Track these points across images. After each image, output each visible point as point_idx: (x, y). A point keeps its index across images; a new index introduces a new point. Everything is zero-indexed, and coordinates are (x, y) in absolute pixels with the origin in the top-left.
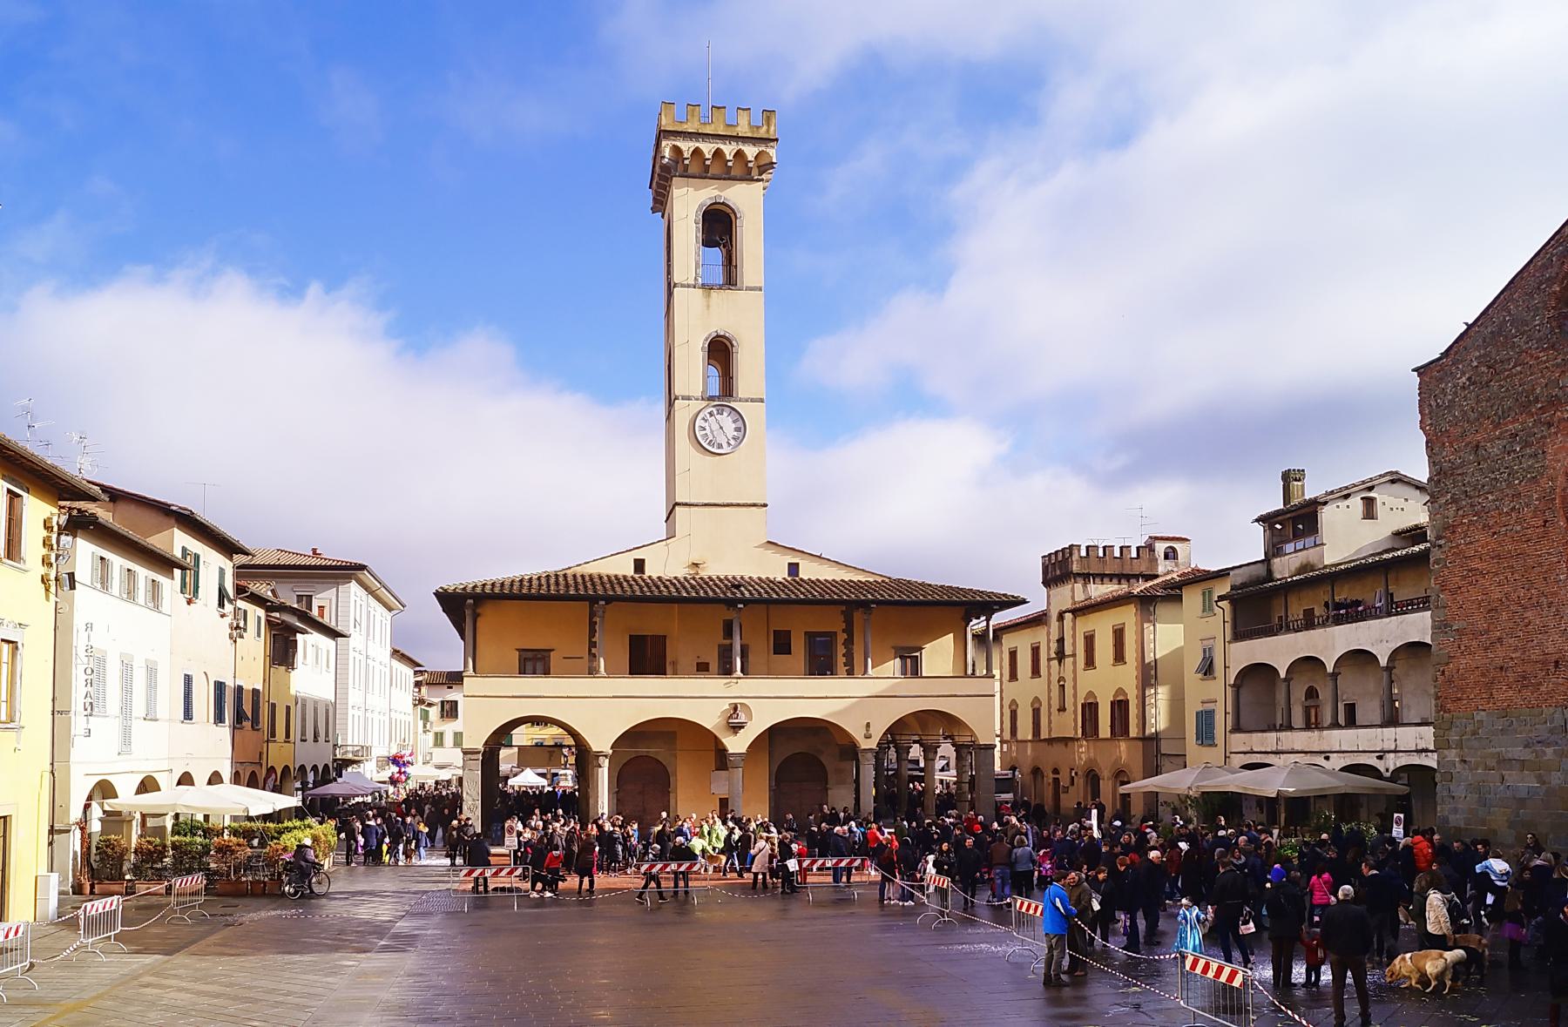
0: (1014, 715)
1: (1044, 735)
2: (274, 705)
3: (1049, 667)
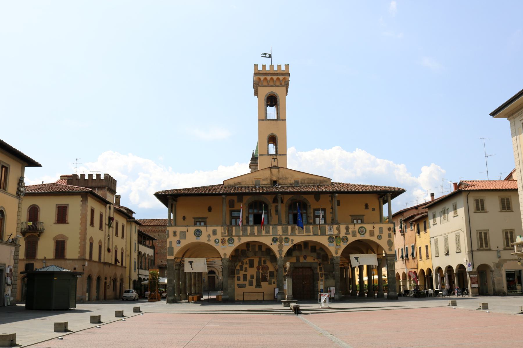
0: (91, 244)
1: (102, 261)
2: (420, 248)
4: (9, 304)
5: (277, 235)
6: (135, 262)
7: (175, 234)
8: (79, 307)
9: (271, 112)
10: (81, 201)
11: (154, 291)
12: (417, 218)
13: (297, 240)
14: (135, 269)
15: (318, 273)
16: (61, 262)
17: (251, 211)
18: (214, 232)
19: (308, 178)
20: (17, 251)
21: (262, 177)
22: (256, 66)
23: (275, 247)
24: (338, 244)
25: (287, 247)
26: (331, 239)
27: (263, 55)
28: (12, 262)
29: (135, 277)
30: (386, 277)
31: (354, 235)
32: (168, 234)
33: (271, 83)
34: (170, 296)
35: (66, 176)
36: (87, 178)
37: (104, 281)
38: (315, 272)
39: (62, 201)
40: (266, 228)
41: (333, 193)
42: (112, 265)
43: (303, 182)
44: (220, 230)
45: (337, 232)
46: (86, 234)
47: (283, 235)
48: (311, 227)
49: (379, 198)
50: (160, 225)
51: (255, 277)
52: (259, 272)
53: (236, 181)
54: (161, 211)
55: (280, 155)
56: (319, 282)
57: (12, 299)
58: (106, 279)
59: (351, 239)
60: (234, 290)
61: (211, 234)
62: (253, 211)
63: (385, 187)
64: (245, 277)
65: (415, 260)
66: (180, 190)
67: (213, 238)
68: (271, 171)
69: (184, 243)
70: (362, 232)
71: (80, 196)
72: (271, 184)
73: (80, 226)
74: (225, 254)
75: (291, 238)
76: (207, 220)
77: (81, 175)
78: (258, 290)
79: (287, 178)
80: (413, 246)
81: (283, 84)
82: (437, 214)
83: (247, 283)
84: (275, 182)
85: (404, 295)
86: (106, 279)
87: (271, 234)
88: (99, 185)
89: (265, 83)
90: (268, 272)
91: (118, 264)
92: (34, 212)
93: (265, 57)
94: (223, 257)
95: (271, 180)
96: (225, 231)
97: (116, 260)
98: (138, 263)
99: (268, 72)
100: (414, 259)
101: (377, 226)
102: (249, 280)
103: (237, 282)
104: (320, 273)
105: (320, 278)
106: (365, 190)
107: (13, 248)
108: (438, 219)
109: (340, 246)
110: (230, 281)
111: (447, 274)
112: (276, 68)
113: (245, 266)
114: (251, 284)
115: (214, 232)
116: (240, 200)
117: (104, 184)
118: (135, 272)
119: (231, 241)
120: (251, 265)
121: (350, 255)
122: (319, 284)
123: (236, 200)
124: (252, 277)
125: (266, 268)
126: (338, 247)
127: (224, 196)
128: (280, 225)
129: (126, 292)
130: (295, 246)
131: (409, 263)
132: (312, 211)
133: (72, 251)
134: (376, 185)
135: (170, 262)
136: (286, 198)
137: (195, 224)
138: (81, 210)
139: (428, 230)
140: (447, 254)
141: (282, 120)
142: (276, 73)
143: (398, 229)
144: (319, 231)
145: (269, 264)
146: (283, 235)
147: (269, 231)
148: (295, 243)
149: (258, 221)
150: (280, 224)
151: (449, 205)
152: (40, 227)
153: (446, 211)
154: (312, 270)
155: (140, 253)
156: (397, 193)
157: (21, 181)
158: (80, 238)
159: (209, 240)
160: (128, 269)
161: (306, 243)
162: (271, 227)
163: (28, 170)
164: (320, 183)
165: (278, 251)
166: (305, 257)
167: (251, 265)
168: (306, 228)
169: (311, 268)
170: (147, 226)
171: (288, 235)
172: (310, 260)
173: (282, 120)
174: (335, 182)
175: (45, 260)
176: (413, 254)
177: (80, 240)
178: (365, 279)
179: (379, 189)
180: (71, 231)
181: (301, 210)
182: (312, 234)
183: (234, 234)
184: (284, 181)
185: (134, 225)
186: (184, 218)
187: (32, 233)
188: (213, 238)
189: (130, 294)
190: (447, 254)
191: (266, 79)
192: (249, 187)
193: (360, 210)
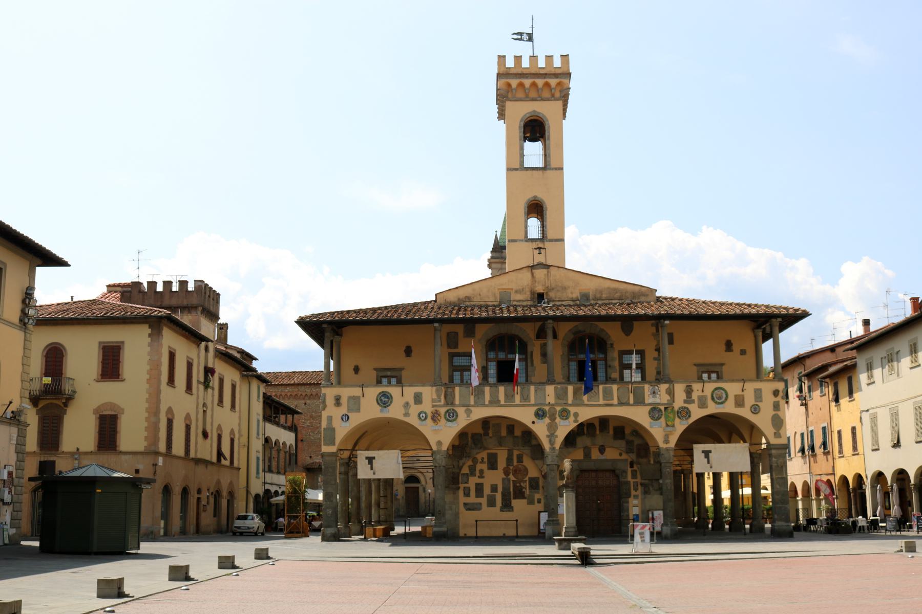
0: (170, 422)
1: (192, 455)
2: (839, 432)
3: (198, 391)
4: (7, 541)
5: (545, 404)
6: (258, 459)
7: (338, 401)
8: (146, 547)
9: (533, 152)
10: (150, 335)
11: (296, 518)
12: (834, 370)
13: (587, 413)
14: (258, 473)
15: (628, 483)
16: (108, 458)
17: (492, 355)
18: (418, 399)
19: (609, 288)
20: (22, 436)
21: (514, 287)
22: (502, 58)
23: (540, 429)
24: (669, 423)
25: (564, 428)
26: (655, 413)
27: (515, 37)
28: (13, 458)
29: (257, 488)
30: (769, 491)
31: (703, 405)
32: (324, 402)
33: (533, 94)
34: (329, 526)
35: (119, 285)
36: (160, 288)
37: (196, 496)
38: (622, 480)
39: (112, 335)
40: (522, 389)
41: (659, 318)
42: (212, 463)
43: (598, 296)
44: (428, 393)
45: (668, 398)
46: (158, 401)
47: (557, 404)
48: (615, 387)
49: (754, 330)
50: (307, 384)
51: (500, 489)
52: (509, 480)
53: (462, 294)
54: (310, 356)
55: (551, 241)
56: (630, 500)
57: (13, 531)
58: (199, 491)
59: (697, 413)
60: (457, 515)
61: (412, 402)
62: (497, 355)
63: (767, 307)
64: (479, 489)
65: (830, 457)
66: (348, 312)
67: (414, 409)
68: (532, 274)
69: (357, 419)
70: (720, 398)
71: (147, 326)
72: (532, 299)
73: (147, 386)
74: (439, 443)
75: (573, 410)
76: (404, 373)
77: (149, 283)
78: (507, 515)
79: (564, 288)
80: (824, 428)
81: (557, 95)
82: (876, 361)
83: (484, 501)
84: (541, 296)
85: (806, 529)
86: (199, 491)
87: (533, 402)
88: (185, 303)
89: (520, 94)
90: (527, 479)
91: (223, 462)
92: (54, 358)
93: (521, 39)
94: (435, 448)
95: (532, 293)
96: (439, 396)
97: (220, 454)
98: (264, 460)
99: (525, 72)
100: (826, 453)
101: (751, 387)
102: (488, 496)
103: (463, 499)
104: (632, 481)
105: (633, 492)
106: (724, 312)
107: (14, 430)
108: (877, 372)
109: (673, 426)
110: (449, 498)
111: (895, 487)
112: (542, 63)
113: (479, 467)
114: (491, 503)
115: (418, 399)
116: (470, 333)
117: (194, 301)
118: (257, 477)
119: (452, 416)
120: (493, 466)
121: (695, 446)
122: (630, 505)
123: (461, 334)
124: (494, 489)
125: (521, 471)
126: (669, 429)
127: (436, 325)
128: (552, 384)
129: (240, 518)
130: (581, 425)
131: (815, 462)
132: (616, 355)
133: (131, 436)
134: (748, 302)
135: (327, 458)
136: (564, 329)
137: (379, 382)
138: (149, 354)
139: (855, 395)
140: (897, 445)
141: (556, 169)
142: (542, 72)
143: (793, 392)
144: (631, 396)
145: (528, 462)
146: (557, 404)
147: (528, 396)
148: (581, 420)
149: (506, 374)
150: (551, 381)
151: (901, 343)
152: (67, 388)
153: (895, 356)
154: (617, 476)
155: (267, 440)
156: (791, 318)
157: (28, 295)
158: (147, 410)
159: (407, 414)
160: (243, 472)
161: (604, 421)
162: (532, 388)
163: (42, 273)
164: (634, 297)
165: (548, 436)
166: (602, 450)
167: (493, 466)
168: (605, 391)
169: (613, 471)
170: (282, 385)
171: (566, 404)
172: (611, 454)
173: (556, 169)
174: (664, 295)
175: (77, 454)
176: (824, 444)
177: (146, 415)
178: (726, 494)
179: (754, 311)
180: (129, 395)
181: (593, 352)
182: (615, 402)
183: (457, 402)
184: (559, 295)
185: (255, 383)
186: (356, 370)
187: (52, 400)
188: (414, 409)
189: (248, 523)
190: (897, 445)
191: (521, 85)
192: (487, 307)
193: (716, 354)
